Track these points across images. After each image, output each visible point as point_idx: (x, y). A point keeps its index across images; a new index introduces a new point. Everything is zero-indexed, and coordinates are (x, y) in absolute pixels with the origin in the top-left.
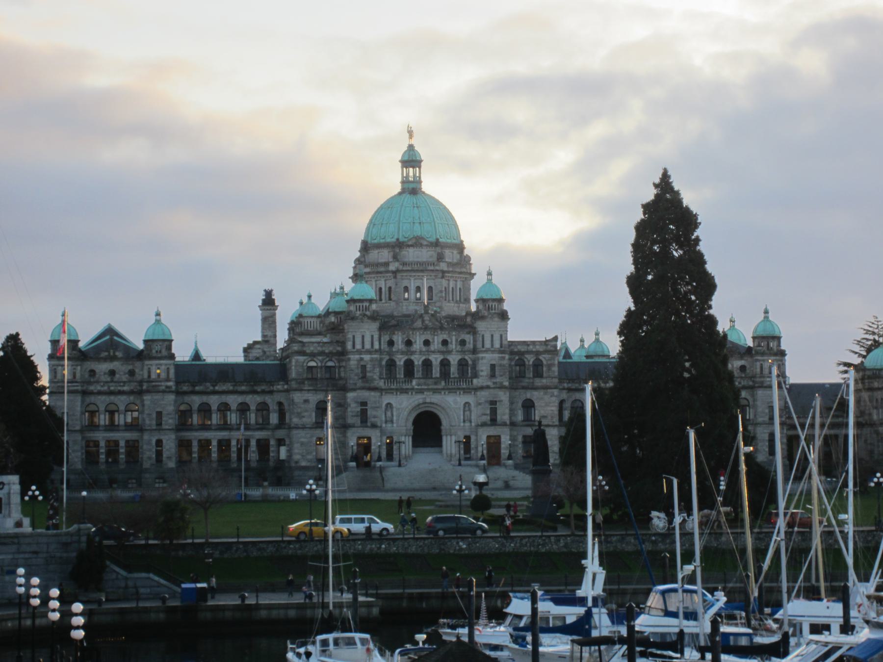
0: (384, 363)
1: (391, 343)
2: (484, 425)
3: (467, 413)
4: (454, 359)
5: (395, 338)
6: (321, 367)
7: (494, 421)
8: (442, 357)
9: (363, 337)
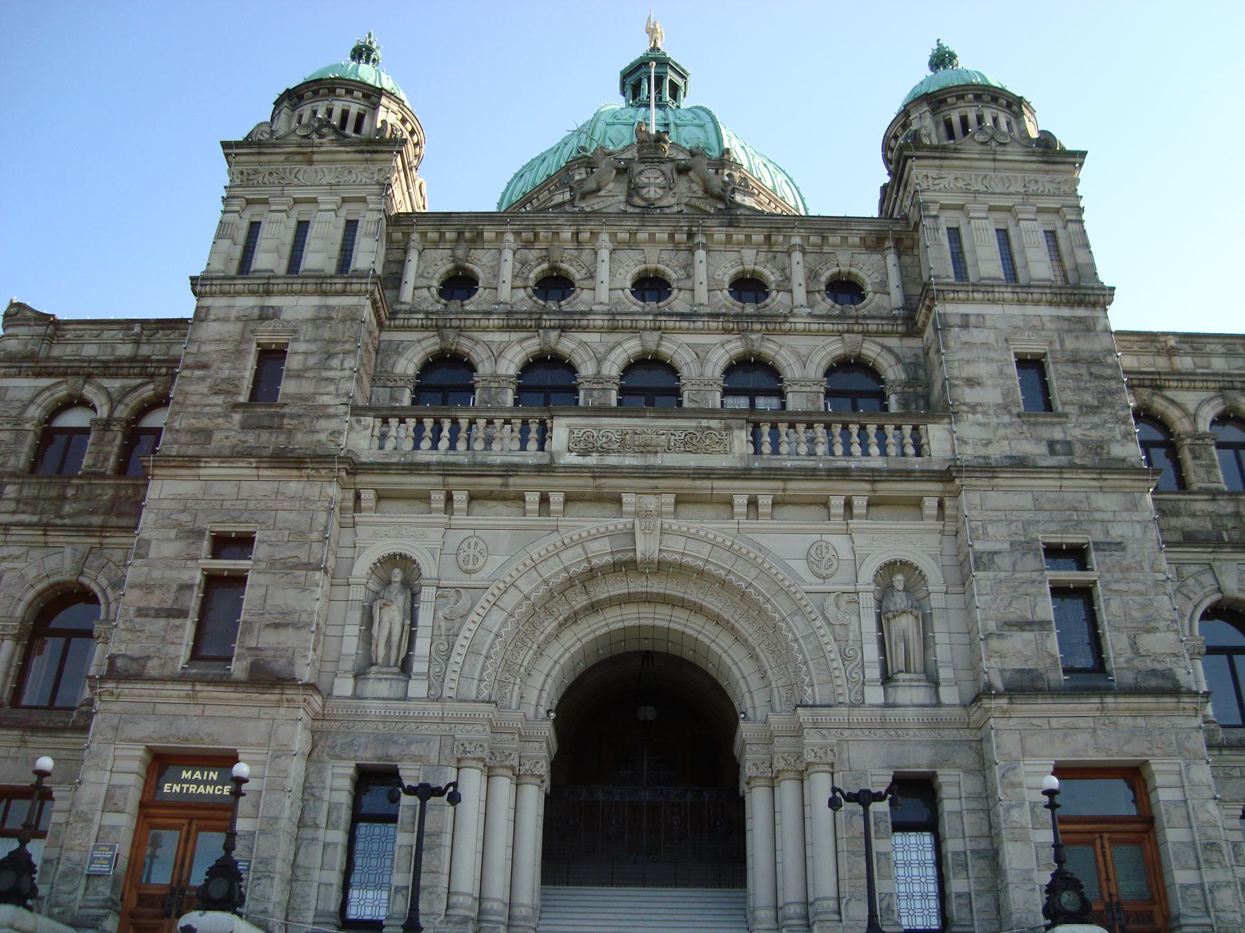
0: (408, 365)
1: (460, 284)
2: (1025, 686)
3: (905, 624)
4: (804, 357)
5: (480, 262)
6: (106, 425)
7: (1090, 675)
8: (735, 347)
9: (302, 228)
